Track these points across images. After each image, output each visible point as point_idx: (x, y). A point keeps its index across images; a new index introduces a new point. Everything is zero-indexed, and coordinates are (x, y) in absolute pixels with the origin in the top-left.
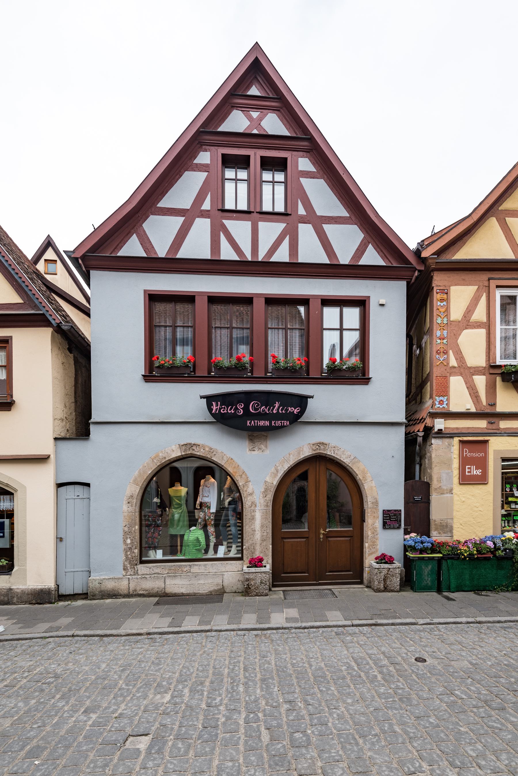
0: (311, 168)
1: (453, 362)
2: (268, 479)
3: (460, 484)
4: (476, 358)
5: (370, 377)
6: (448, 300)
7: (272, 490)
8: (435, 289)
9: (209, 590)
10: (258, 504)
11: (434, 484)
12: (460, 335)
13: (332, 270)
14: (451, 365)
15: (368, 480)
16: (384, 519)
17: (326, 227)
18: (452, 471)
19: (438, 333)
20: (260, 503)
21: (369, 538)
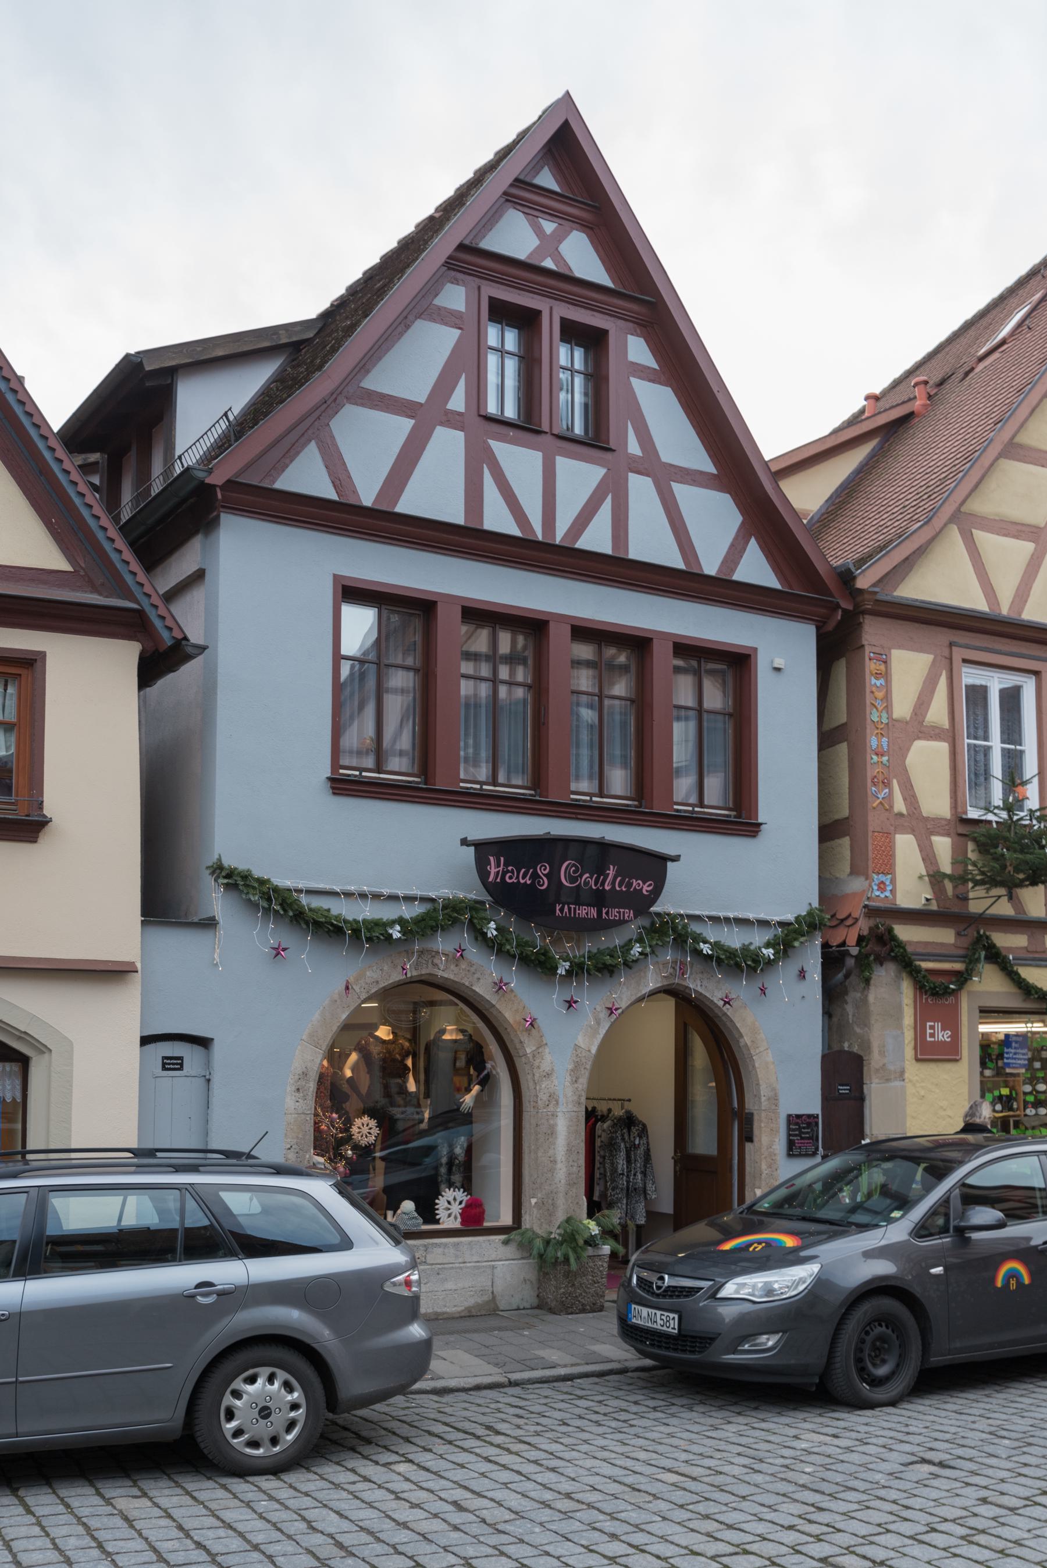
0: (651, 362)
1: (899, 805)
2: (581, 1040)
3: (917, 1060)
4: (936, 803)
5: (760, 821)
6: (886, 675)
7: (588, 1067)
8: (867, 649)
9: (467, 1304)
10: (562, 1100)
11: (875, 1060)
12: (908, 750)
13: (684, 584)
14: (896, 810)
15: (761, 1049)
16: (789, 1135)
17: (678, 488)
18: (903, 1033)
19: (874, 742)
20: (565, 1096)
21: (764, 1175)
